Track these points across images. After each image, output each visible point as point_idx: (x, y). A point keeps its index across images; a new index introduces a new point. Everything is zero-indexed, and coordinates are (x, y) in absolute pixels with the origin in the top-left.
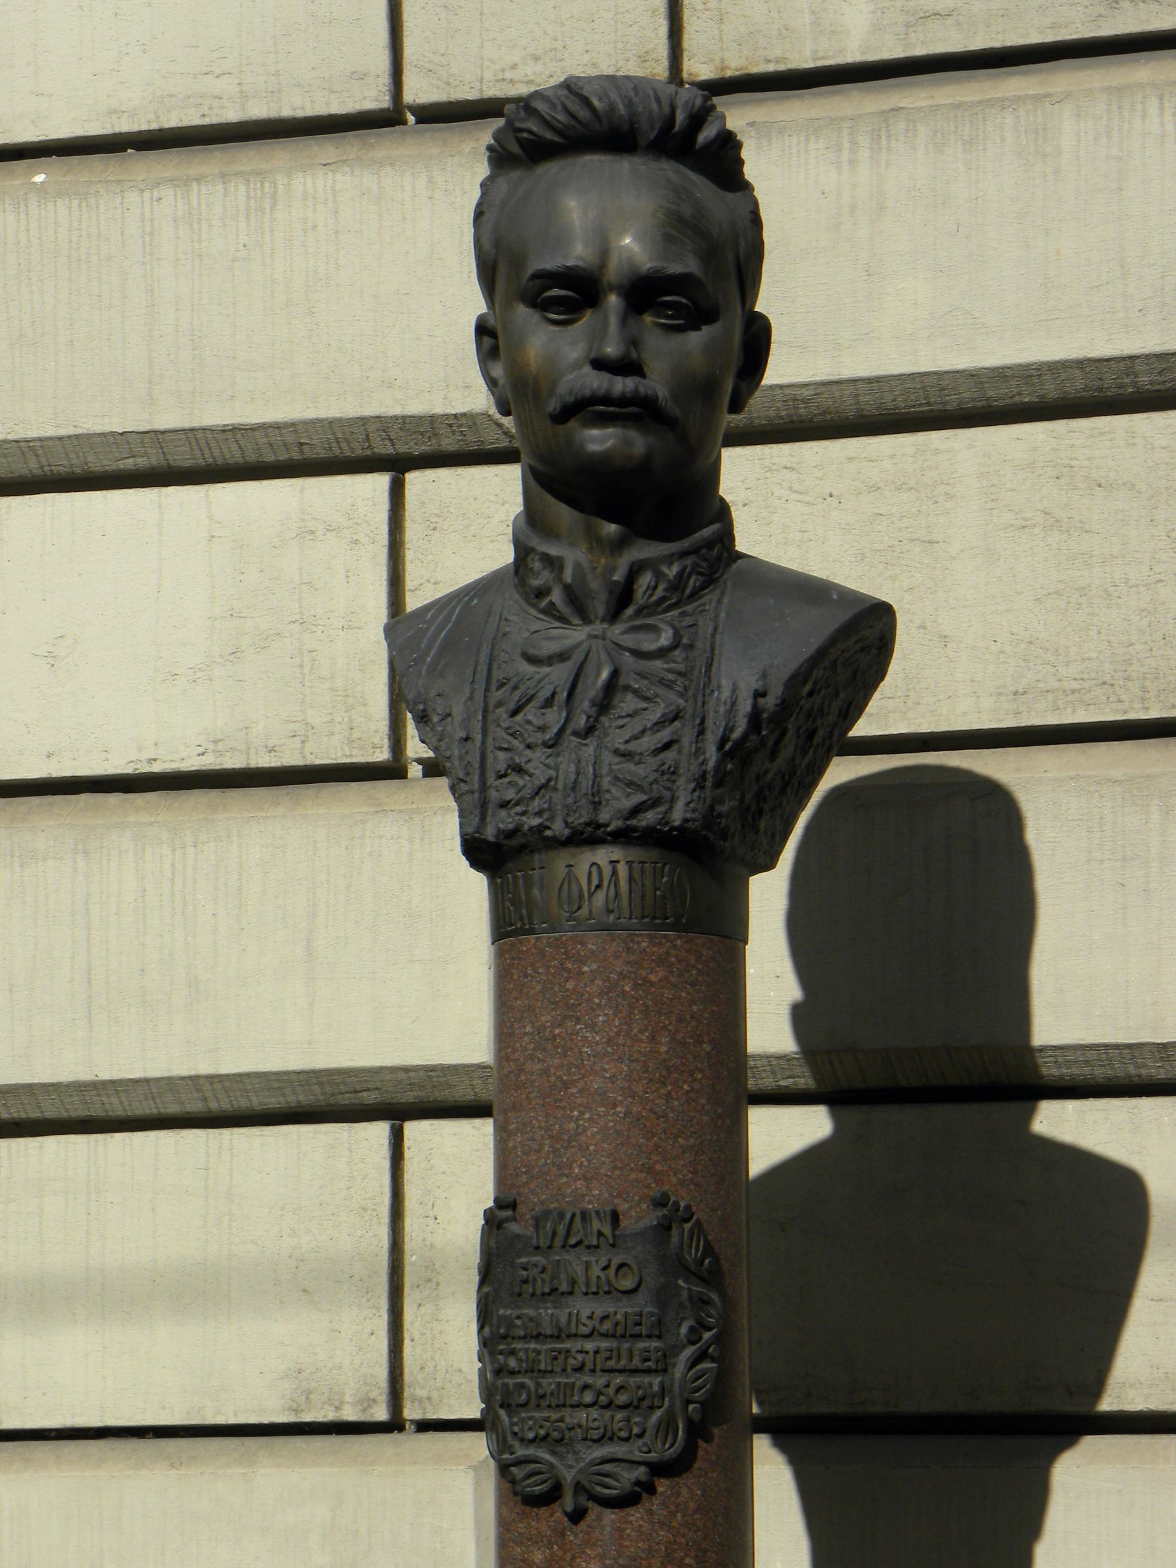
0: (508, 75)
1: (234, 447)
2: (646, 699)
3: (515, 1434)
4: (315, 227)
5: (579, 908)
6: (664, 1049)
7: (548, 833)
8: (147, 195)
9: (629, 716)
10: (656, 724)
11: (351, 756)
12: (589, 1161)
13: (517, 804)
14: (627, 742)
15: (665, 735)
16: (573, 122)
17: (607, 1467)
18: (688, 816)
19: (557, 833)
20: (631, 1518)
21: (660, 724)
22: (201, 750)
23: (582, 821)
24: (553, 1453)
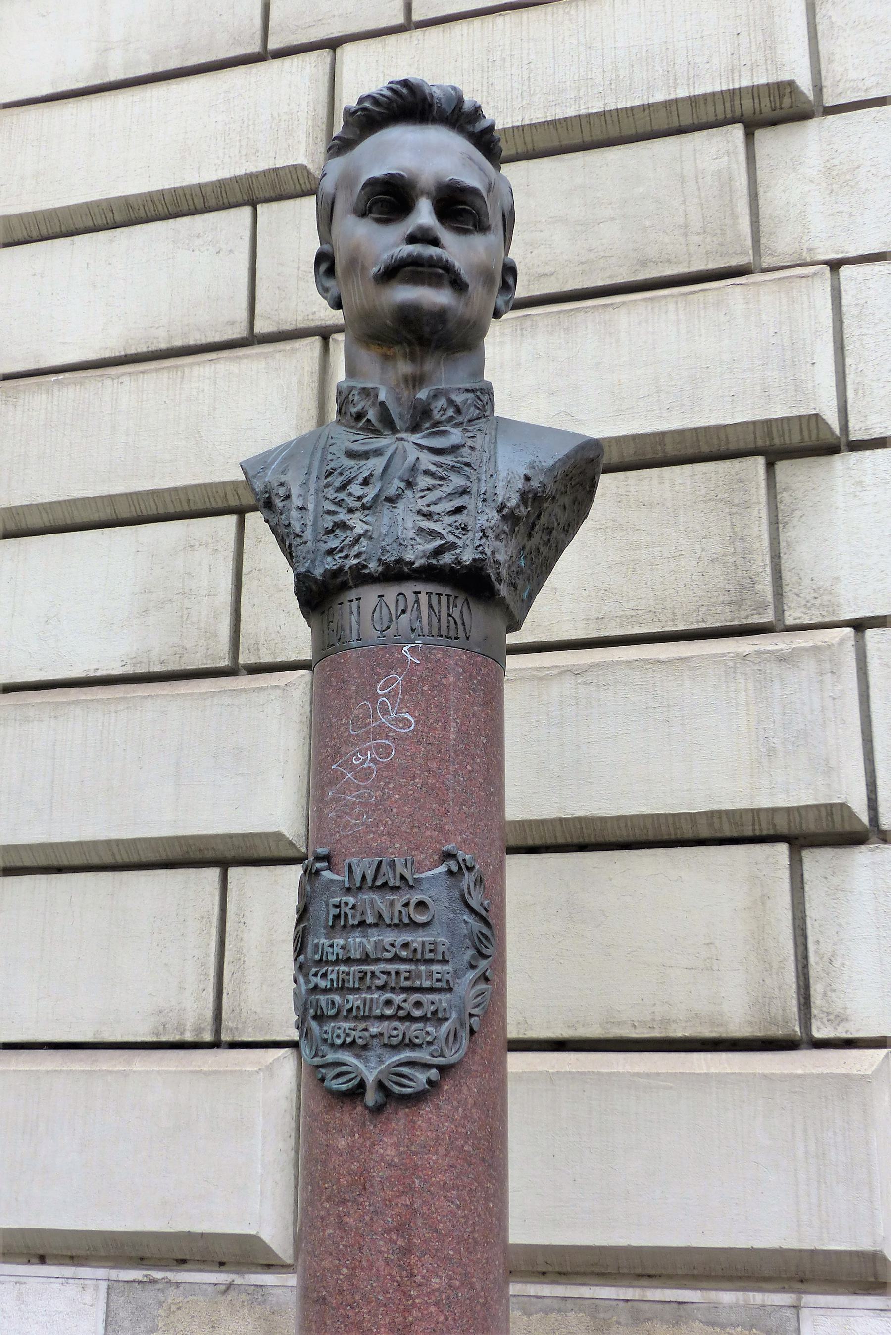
0: (311, 317)
1: (153, 504)
2: (442, 478)
3: (325, 1040)
4: (203, 391)
5: (388, 627)
6: (453, 736)
7: (366, 571)
8: (115, 381)
9: (428, 489)
10: (450, 494)
11: (207, 664)
12: (392, 821)
13: (341, 551)
14: (428, 506)
15: (458, 502)
16: (395, 97)
17: (405, 1070)
18: (477, 557)
19: (373, 570)
20: (422, 1112)
21: (451, 496)
22: (123, 663)
23: (393, 559)
24: (358, 1056)
